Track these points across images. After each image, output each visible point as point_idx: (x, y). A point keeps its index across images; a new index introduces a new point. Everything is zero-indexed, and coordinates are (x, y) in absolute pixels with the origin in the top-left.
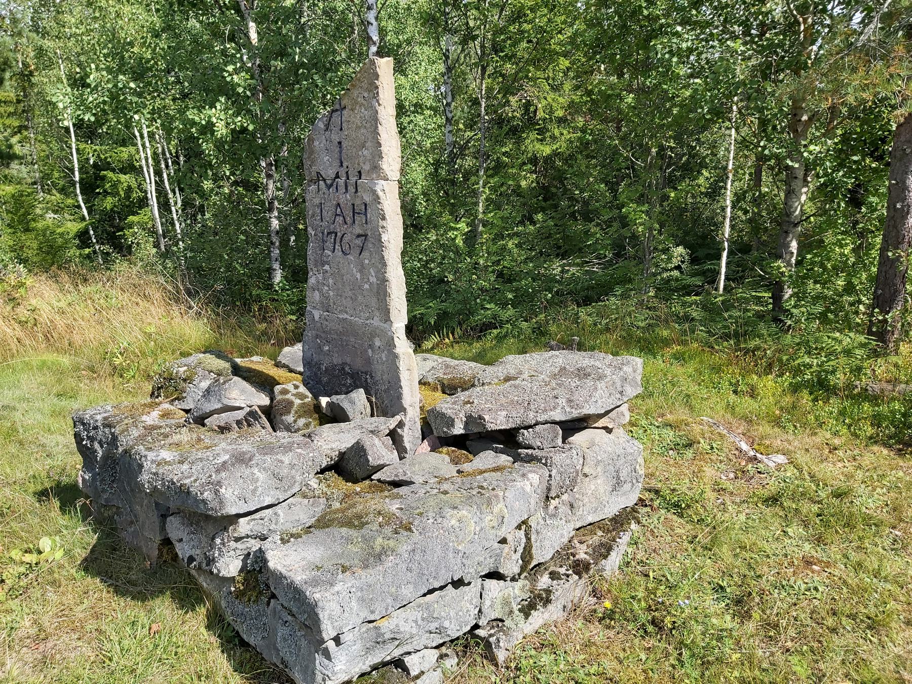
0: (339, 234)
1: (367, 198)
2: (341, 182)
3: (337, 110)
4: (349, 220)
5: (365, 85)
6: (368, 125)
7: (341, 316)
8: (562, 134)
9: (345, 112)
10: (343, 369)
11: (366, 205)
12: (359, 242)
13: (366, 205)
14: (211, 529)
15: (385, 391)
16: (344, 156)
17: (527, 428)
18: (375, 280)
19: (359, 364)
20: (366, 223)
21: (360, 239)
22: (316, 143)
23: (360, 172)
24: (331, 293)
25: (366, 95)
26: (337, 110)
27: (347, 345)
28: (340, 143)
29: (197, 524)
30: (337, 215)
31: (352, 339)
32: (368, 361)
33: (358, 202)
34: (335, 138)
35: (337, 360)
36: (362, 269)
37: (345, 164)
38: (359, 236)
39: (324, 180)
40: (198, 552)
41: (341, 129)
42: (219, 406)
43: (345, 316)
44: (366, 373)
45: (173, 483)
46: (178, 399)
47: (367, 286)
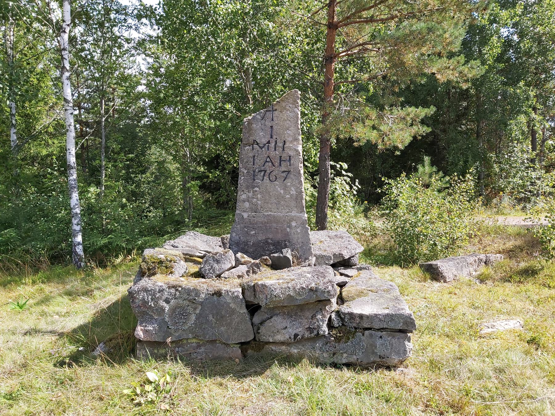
0: (268, 171)
1: (291, 153)
4: (277, 164)
5: (291, 101)
6: (292, 120)
7: (266, 214)
8: (54, 143)
9: (276, 112)
10: (267, 242)
11: (290, 157)
12: (284, 175)
13: (290, 157)
14: (309, 314)
15: (300, 248)
17: (353, 257)
18: (295, 193)
19: (279, 237)
20: (290, 165)
21: (285, 173)
22: (254, 126)
23: (284, 141)
24: (259, 202)
25: (291, 106)
27: (270, 228)
28: (272, 127)
29: (296, 314)
30: (266, 162)
31: (275, 225)
32: (287, 234)
33: (284, 155)
34: (269, 124)
35: (261, 237)
36: (285, 188)
37: (274, 137)
38: (284, 172)
39: (258, 144)
40: (300, 329)
41: (273, 120)
42: (230, 266)
43: (270, 213)
44: (285, 241)
45: (303, 288)
46: (171, 273)
47: (288, 196)
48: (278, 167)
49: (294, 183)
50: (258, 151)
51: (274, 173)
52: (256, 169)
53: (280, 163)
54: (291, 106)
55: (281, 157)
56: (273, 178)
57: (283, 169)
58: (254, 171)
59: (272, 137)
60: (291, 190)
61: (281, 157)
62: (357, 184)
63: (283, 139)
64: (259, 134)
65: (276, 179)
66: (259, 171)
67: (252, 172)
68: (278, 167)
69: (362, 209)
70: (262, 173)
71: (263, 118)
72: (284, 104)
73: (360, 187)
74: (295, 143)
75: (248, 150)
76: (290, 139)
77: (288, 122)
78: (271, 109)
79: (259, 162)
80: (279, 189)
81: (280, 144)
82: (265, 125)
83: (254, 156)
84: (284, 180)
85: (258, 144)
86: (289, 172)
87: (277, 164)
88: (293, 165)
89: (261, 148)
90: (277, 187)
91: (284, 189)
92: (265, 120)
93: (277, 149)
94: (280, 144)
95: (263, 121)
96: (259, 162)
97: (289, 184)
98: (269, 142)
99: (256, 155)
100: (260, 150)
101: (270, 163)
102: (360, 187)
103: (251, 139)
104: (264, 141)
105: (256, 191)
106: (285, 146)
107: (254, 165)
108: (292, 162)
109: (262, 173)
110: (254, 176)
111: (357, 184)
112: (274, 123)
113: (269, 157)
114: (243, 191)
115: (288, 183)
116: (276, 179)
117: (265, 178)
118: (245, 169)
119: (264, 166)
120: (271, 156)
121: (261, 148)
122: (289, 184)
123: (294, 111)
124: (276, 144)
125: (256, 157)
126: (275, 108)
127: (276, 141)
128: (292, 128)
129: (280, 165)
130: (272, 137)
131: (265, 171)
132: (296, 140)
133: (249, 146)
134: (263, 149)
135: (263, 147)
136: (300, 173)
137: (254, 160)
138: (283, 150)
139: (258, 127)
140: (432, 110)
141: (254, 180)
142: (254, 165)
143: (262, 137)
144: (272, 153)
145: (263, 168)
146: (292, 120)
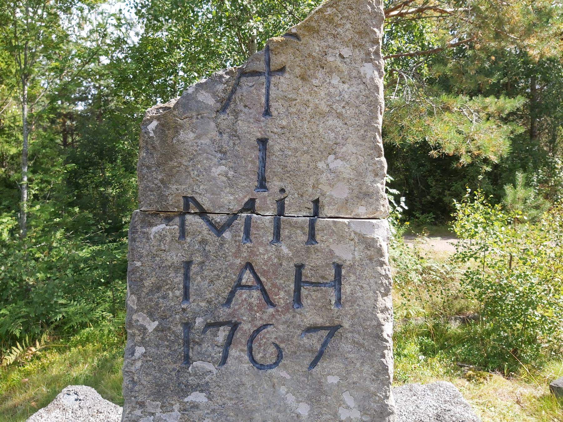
1: (346, 253)
2: (265, 219)
3: (255, 73)
4: (282, 297)
5: (347, 30)
6: (349, 112)
9: (282, 83)
12: (314, 341)
13: (338, 267)
16: (273, 166)
22: (187, 136)
25: (346, 52)
26: (255, 73)
28: (263, 142)
30: (239, 285)
34: (250, 128)
37: (274, 184)
38: (312, 329)
39: (203, 213)
41: (267, 113)
48: (287, 309)
49: (355, 377)
50: (203, 242)
51: (270, 334)
52: (196, 315)
53: (298, 290)
54: (346, 52)
55: (299, 268)
56: (265, 354)
57: (310, 316)
58: (188, 326)
59: (262, 184)
60: (341, 402)
61: (299, 268)
62: (403, 204)
63: (311, 193)
64: (208, 170)
65: (280, 356)
66: (208, 326)
67: (179, 329)
68: (287, 309)
69: (402, 232)
70: (222, 334)
71: (225, 104)
72: (316, 46)
73: (406, 208)
74: (361, 210)
75: (162, 237)
76: (341, 192)
77: (332, 121)
78: (261, 66)
79: (209, 287)
80: (291, 399)
81: (298, 215)
82: (234, 134)
83: (188, 264)
84: (314, 364)
85: (203, 213)
86: (333, 330)
87: (282, 297)
88: (353, 301)
89: (219, 230)
90: (283, 390)
91: (312, 400)
92: (236, 114)
93: (285, 233)
94: (298, 215)
95: (226, 119)
96: (209, 287)
97: (333, 380)
98: (250, 206)
99: (198, 259)
100: (211, 236)
101: (256, 293)
102: (406, 208)
103: (175, 193)
104: (232, 200)
105: (195, 406)
106: (320, 222)
107: (186, 296)
108: (347, 289)
109: (222, 334)
110: (187, 342)
111: (403, 204)
112: (270, 128)
113: (249, 266)
114: (142, 405)
115: (331, 375)
116: (280, 356)
117: (233, 352)
118: (151, 315)
119: (229, 301)
120: (259, 263)
121: (219, 230)
122: (333, 380)
123: (360, 78)
124: (281, 212)
125: (194, 268)
126: (277, 61)
127: (281, 204)
128: (349, 148)
129: (298, 300)
130: (262, 184)
131: (235, 326)
132: (366, 195)
133: (168, 220)
134: (227, 235)
135: (228, 225)
136: (378, 337)
137: (187, 277)
138: (312, 237)
139: (205, 141)
140: (519, 102)
141: (187, 360)
142: (186, 296)
143: (220, 184)
144: (265, 254)
145: (223, 313)
146: (349, 112)
